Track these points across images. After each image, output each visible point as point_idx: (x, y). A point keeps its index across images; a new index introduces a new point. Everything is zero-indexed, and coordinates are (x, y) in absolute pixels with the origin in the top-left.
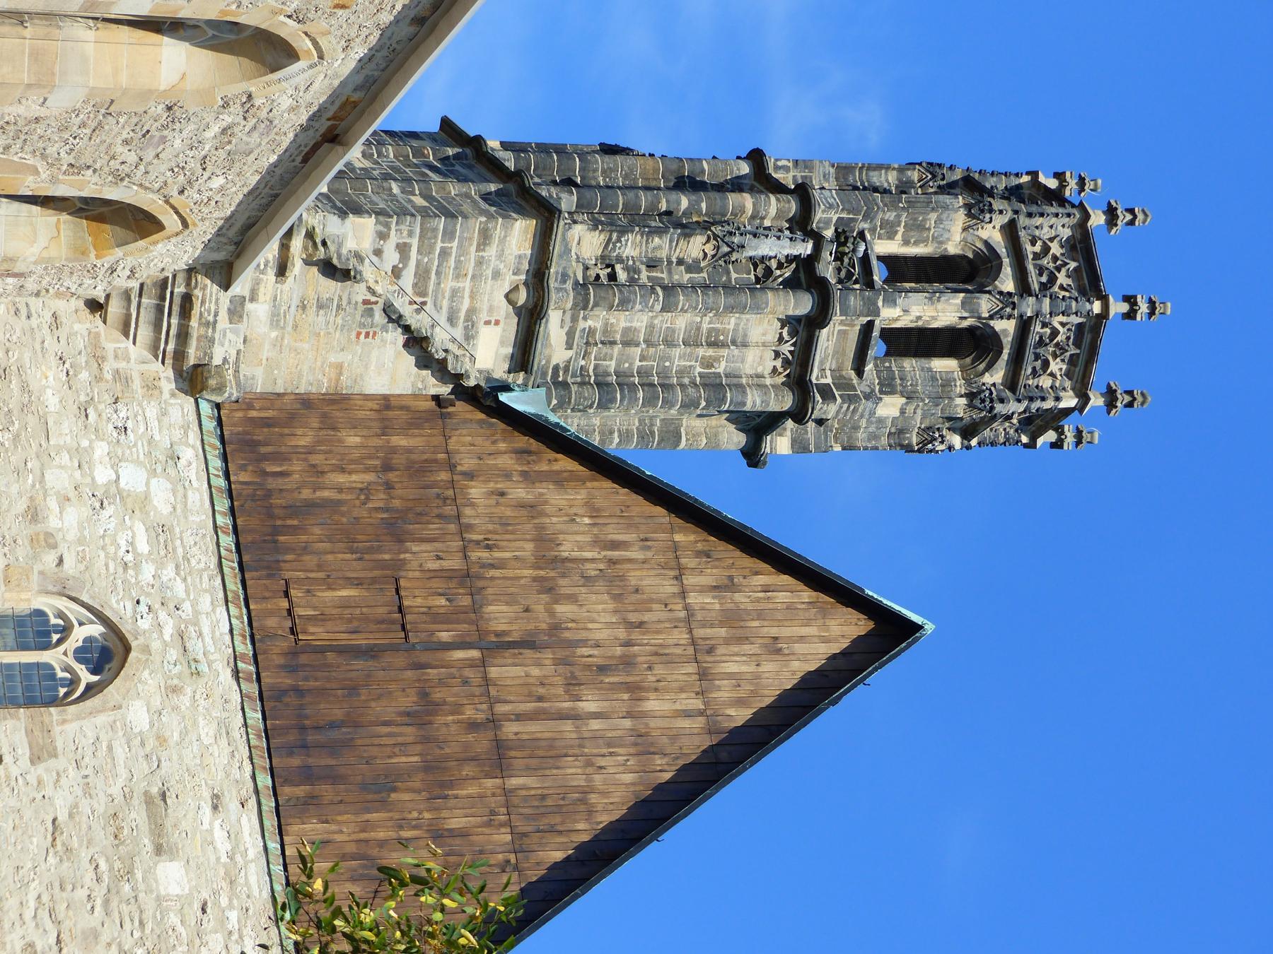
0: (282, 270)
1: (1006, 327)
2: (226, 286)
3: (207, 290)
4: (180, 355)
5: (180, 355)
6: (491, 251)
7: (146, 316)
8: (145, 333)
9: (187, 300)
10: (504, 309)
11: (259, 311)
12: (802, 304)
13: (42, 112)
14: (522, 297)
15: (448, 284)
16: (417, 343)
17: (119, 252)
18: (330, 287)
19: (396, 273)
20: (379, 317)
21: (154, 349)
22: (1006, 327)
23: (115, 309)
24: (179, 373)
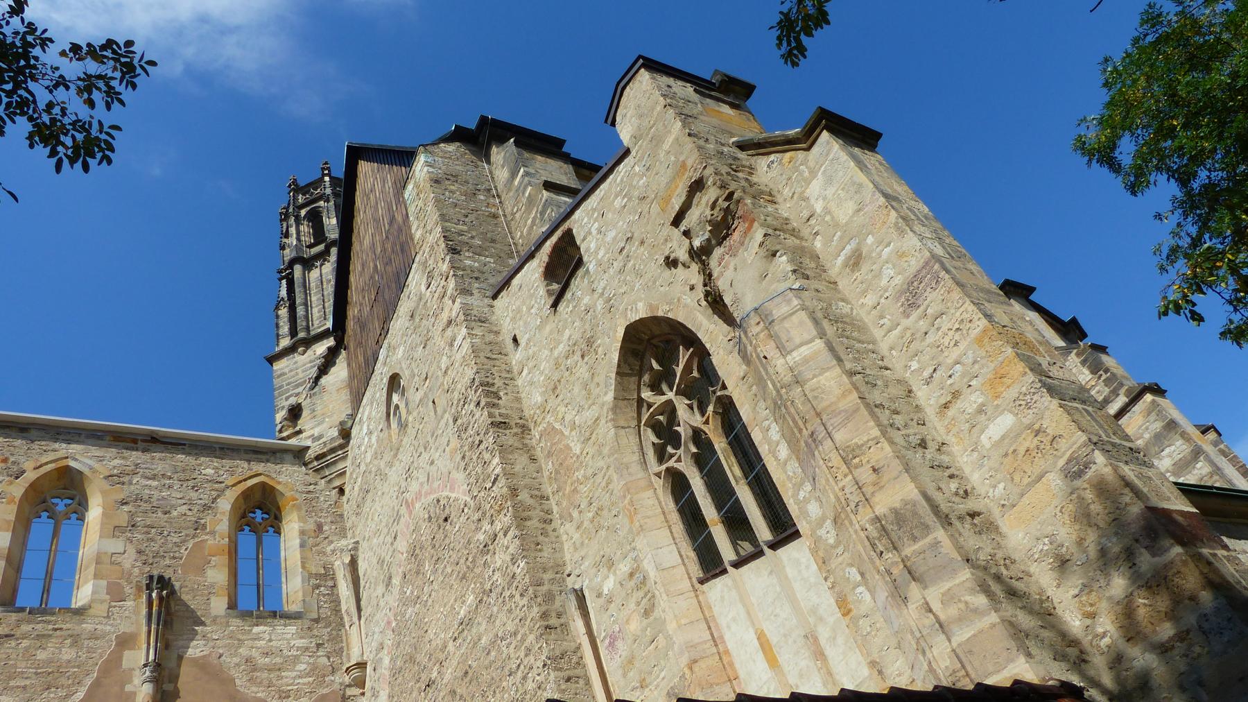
0: (300, 432)
1: (303, 212)
2: (308, 448)
3: (311, 454)
4: (342, 447)
5: (342, 447)
6: (286, 370)
7: (333, 469)
8: (340, 466)
9: (318, 458)
10: (309, 352)
11: (316, 432)
12: (298, 269)
13: (131, 551)
14: (301, 349)
15: (301, 375)
16: (324, 369)
17: (288, 494)
18: (305, 413)
19: (297, 395)
20: (316, 389)
21: (344, 458)
22: (303, 212)
23: (337, 483)
24: (348, 442)
